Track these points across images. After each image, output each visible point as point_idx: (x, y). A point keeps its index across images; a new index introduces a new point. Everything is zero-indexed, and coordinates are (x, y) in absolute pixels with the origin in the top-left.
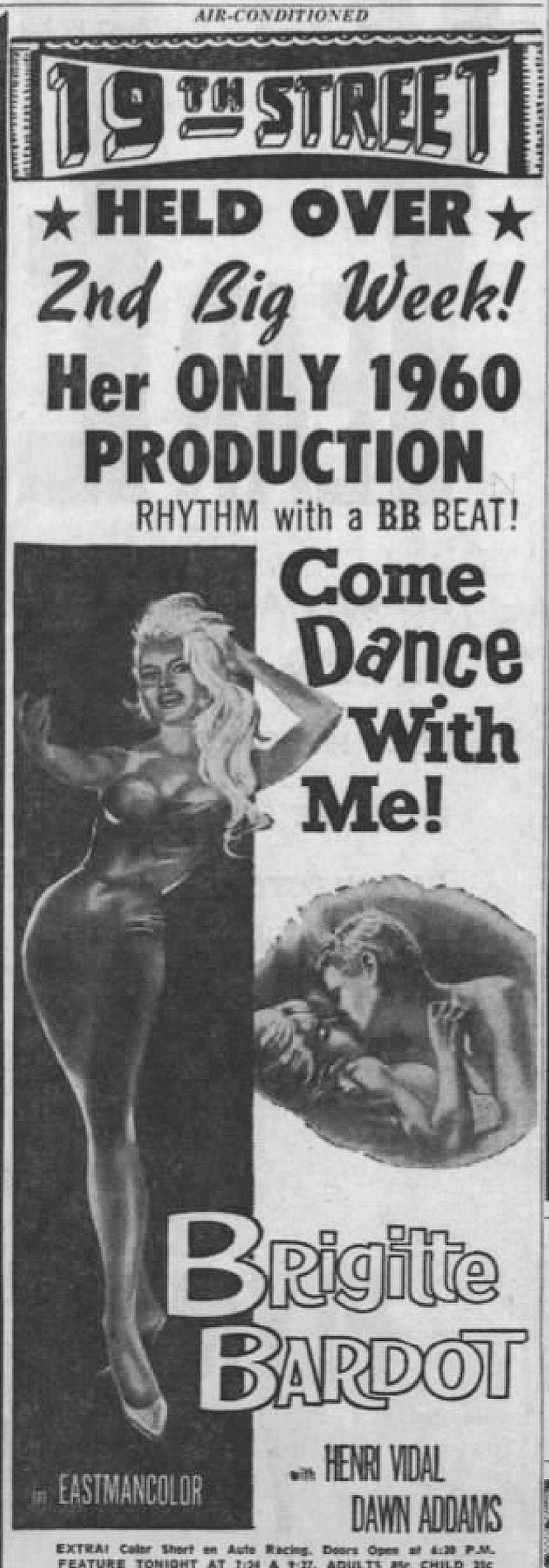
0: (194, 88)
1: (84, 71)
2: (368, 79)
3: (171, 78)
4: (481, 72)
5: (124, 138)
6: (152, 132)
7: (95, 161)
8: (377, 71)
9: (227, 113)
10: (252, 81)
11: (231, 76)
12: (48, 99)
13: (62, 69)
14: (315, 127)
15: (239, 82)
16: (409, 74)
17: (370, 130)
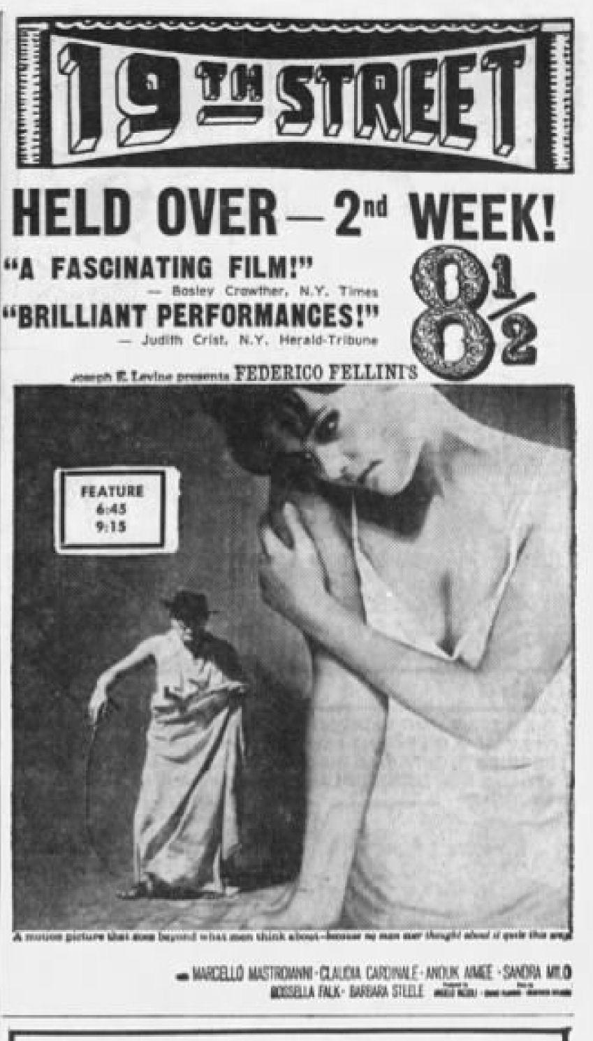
0: (213, 74)
1: (97, 51)
2: (389, 70)
3: (188, 63)
4: (507, 62)
5: (139, 124)
6: (169, 117)
7: (107, 146)
8: (400, 61)
9: (246, 102)
10: (272, 68)
11: (250, 62)
12: (58, 81)
13: (75, 51)
14: (337, 117)
15: (258, 69)
16: (432, 65)
17: (393, 122)
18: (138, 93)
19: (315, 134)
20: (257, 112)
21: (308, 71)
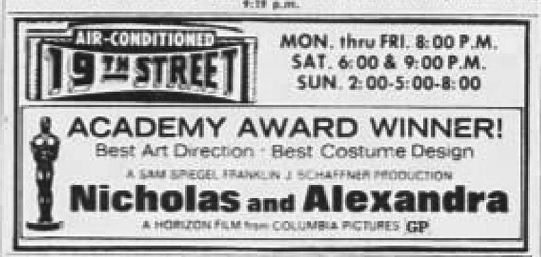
0: (108, 61)
3: (98, 56)
4: (230, 56)
5: (77, 82)
6: (89, 80)
7: (64, 92)
8: (187, 54)
9: (122, 72)
10: (133, 58)
11: (124, 55)
13: (52, 51)
14: (159, 79)
15: (127, 59)
17: (183, 81)
18: (77, 69)
19: (149, 86)
20: (125, 77)
21: (147, 59)
